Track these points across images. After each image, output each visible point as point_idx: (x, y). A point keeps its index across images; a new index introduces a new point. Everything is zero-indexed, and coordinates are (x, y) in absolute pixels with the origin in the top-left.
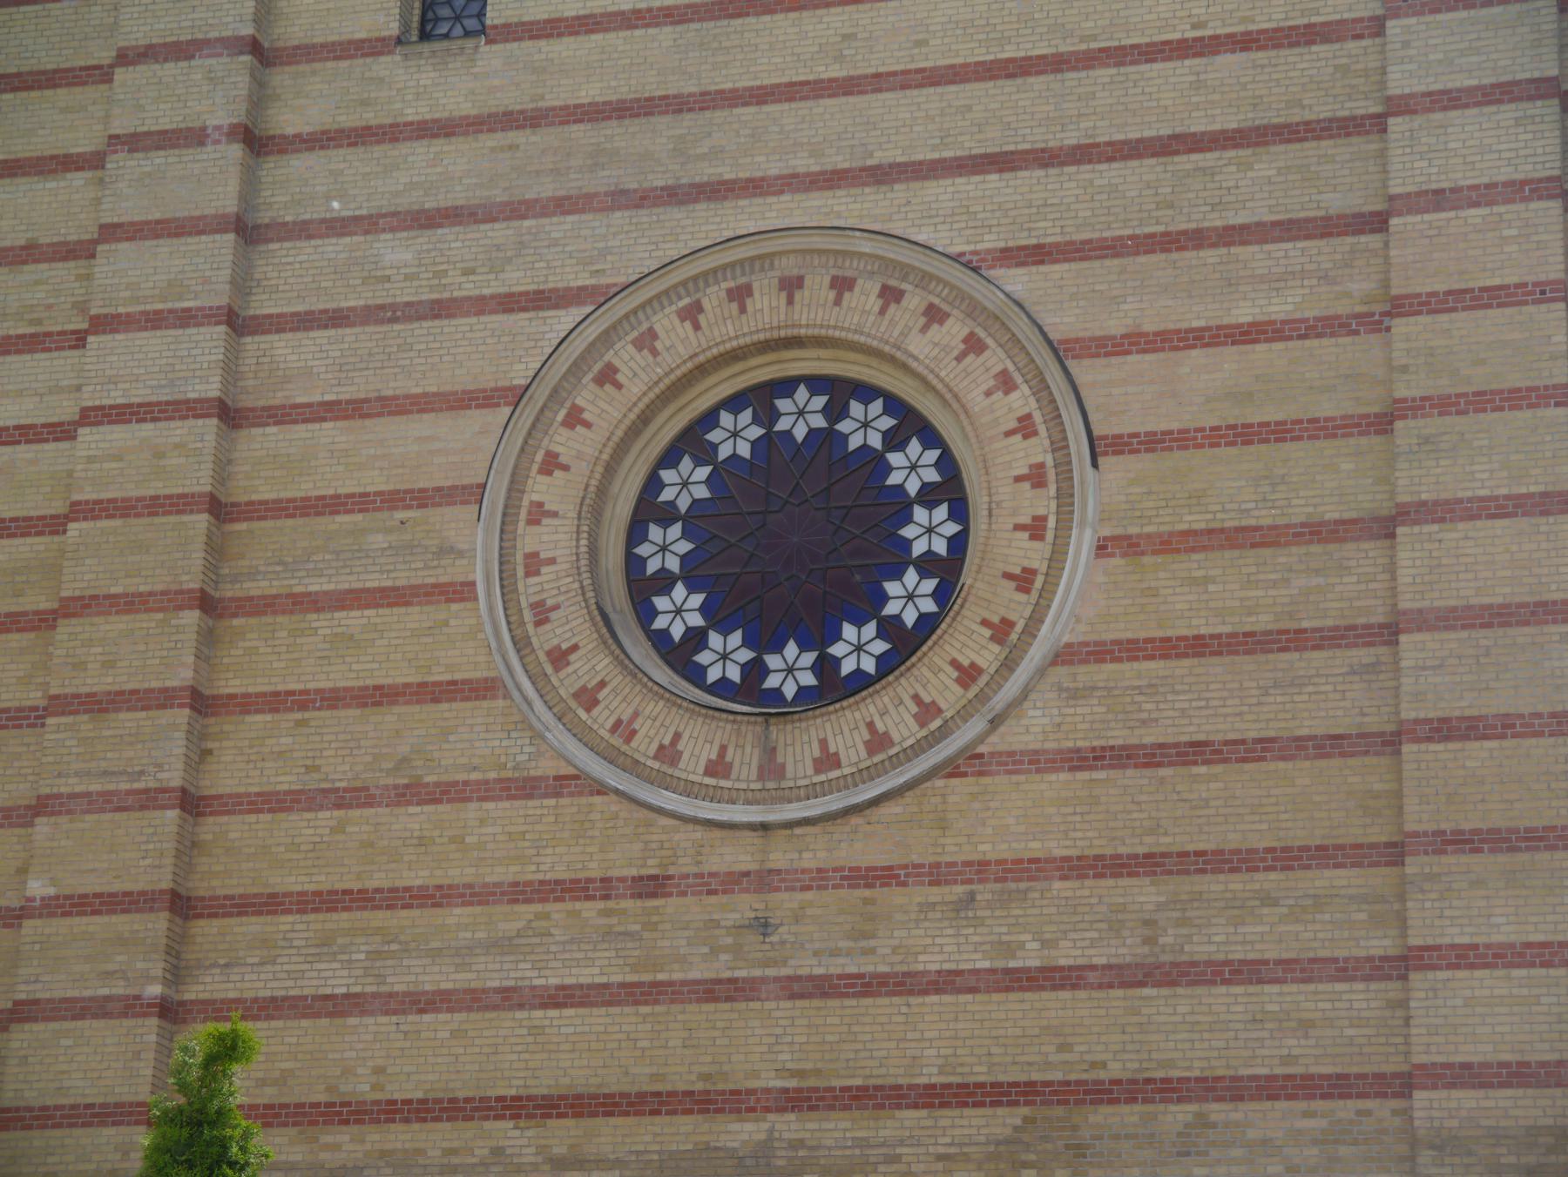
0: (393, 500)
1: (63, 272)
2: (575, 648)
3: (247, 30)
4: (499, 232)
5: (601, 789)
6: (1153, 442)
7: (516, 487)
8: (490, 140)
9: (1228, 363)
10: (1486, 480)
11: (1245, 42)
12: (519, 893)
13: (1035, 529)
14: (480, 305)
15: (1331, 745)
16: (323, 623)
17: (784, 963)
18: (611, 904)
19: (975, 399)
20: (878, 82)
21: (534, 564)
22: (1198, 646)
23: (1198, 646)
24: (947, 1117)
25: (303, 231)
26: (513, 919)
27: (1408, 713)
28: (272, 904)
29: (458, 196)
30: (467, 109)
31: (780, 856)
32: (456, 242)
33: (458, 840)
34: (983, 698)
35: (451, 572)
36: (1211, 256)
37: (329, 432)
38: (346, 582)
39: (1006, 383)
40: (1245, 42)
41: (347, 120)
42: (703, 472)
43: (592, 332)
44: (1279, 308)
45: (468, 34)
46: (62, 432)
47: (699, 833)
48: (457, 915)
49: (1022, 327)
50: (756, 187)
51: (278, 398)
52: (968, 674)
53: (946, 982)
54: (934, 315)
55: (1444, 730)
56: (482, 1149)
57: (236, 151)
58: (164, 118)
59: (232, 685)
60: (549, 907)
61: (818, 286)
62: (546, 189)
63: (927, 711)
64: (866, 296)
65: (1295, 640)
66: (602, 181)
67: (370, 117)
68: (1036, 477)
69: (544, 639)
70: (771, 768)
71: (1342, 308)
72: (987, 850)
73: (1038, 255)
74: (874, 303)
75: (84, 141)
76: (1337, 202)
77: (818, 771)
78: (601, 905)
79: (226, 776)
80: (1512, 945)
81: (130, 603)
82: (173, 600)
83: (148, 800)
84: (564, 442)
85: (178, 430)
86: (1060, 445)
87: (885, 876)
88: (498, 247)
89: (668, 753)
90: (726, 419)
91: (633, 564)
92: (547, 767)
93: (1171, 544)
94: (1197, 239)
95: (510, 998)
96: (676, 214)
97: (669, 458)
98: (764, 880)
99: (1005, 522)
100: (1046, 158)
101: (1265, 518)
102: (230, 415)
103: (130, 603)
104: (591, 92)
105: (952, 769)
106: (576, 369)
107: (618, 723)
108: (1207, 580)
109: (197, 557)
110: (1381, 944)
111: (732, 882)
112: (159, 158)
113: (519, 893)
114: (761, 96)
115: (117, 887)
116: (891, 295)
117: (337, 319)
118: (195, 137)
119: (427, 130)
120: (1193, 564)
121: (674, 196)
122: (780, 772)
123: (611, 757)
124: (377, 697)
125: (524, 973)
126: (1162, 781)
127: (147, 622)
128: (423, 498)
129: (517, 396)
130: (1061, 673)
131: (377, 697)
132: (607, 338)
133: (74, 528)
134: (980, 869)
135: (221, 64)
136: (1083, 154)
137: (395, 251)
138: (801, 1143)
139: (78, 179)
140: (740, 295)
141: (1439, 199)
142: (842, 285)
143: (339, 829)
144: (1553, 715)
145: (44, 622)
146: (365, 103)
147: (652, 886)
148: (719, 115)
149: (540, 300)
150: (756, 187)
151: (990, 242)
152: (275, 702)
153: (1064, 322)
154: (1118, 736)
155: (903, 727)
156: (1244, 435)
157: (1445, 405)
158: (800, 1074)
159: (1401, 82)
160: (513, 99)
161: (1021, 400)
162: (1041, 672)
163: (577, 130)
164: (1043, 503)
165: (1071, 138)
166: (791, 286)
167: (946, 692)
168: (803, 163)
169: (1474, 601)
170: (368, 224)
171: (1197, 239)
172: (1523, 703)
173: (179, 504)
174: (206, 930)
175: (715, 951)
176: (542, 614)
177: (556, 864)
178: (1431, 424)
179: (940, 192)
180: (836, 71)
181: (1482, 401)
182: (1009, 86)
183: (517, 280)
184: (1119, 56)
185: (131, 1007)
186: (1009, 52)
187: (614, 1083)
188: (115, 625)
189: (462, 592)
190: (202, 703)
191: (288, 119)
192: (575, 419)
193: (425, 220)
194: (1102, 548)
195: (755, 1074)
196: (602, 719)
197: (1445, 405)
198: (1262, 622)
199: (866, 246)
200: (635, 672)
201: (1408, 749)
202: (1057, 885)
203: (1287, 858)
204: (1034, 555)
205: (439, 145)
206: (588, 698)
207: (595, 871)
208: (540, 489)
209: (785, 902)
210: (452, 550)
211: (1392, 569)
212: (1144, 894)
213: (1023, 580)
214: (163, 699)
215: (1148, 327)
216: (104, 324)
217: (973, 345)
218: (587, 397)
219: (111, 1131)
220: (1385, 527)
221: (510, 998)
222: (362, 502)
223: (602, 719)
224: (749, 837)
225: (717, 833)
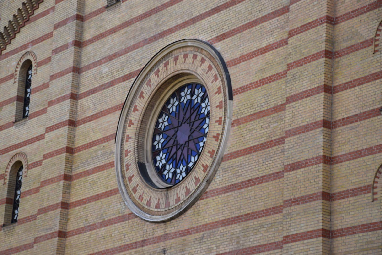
2: (133, 176)
4: (123, 58)
7: (124, 133)
8: (122, 31)
18: (137, 249)
32: (116, 62)
33: (110, 236)
36: (258, 27)
37: (92, 124)
41: (98, 33)
47: (154, 226)
50: (170, 31)
58: (61, 43)
59: (73, 199)
67: (102, 31)
70: (168, 204)
73: (222, 37)
74: (191, 60)
77: (176, 203)
78: (134, 250)
80: (304, 233)
86: (225, 95)
87: (186, 233)
88: (123, 63)
91: (153, 147)
98: (165, 237)
107: (140, 196)
108: (254, 129)
111: (159, 239)
118: (65, 47)
120: (250, 125)
121: (155, 38)
124: (98, 197)
126: (242, 193)
131: (98, 197)
137: (105, 69)
140: (166, 65)
143: (90, 237)
144: (316, 158)
148: (164, 12)
150: (170, 31)
151: (215, 35)
154: (234, 181)
160: (127, 18)
166: (176, 59)
169: (301, 125)
179: (204, 22)
183: (126, 71)
189: (111, 165)
193: (110, 58)
196: (136, 196)
198: (264, 140)
199: (190, 44)
202: (220, 229)
203: (267, 212)
212: (237, 228)
213: (216, 137)
225: (157, 225)
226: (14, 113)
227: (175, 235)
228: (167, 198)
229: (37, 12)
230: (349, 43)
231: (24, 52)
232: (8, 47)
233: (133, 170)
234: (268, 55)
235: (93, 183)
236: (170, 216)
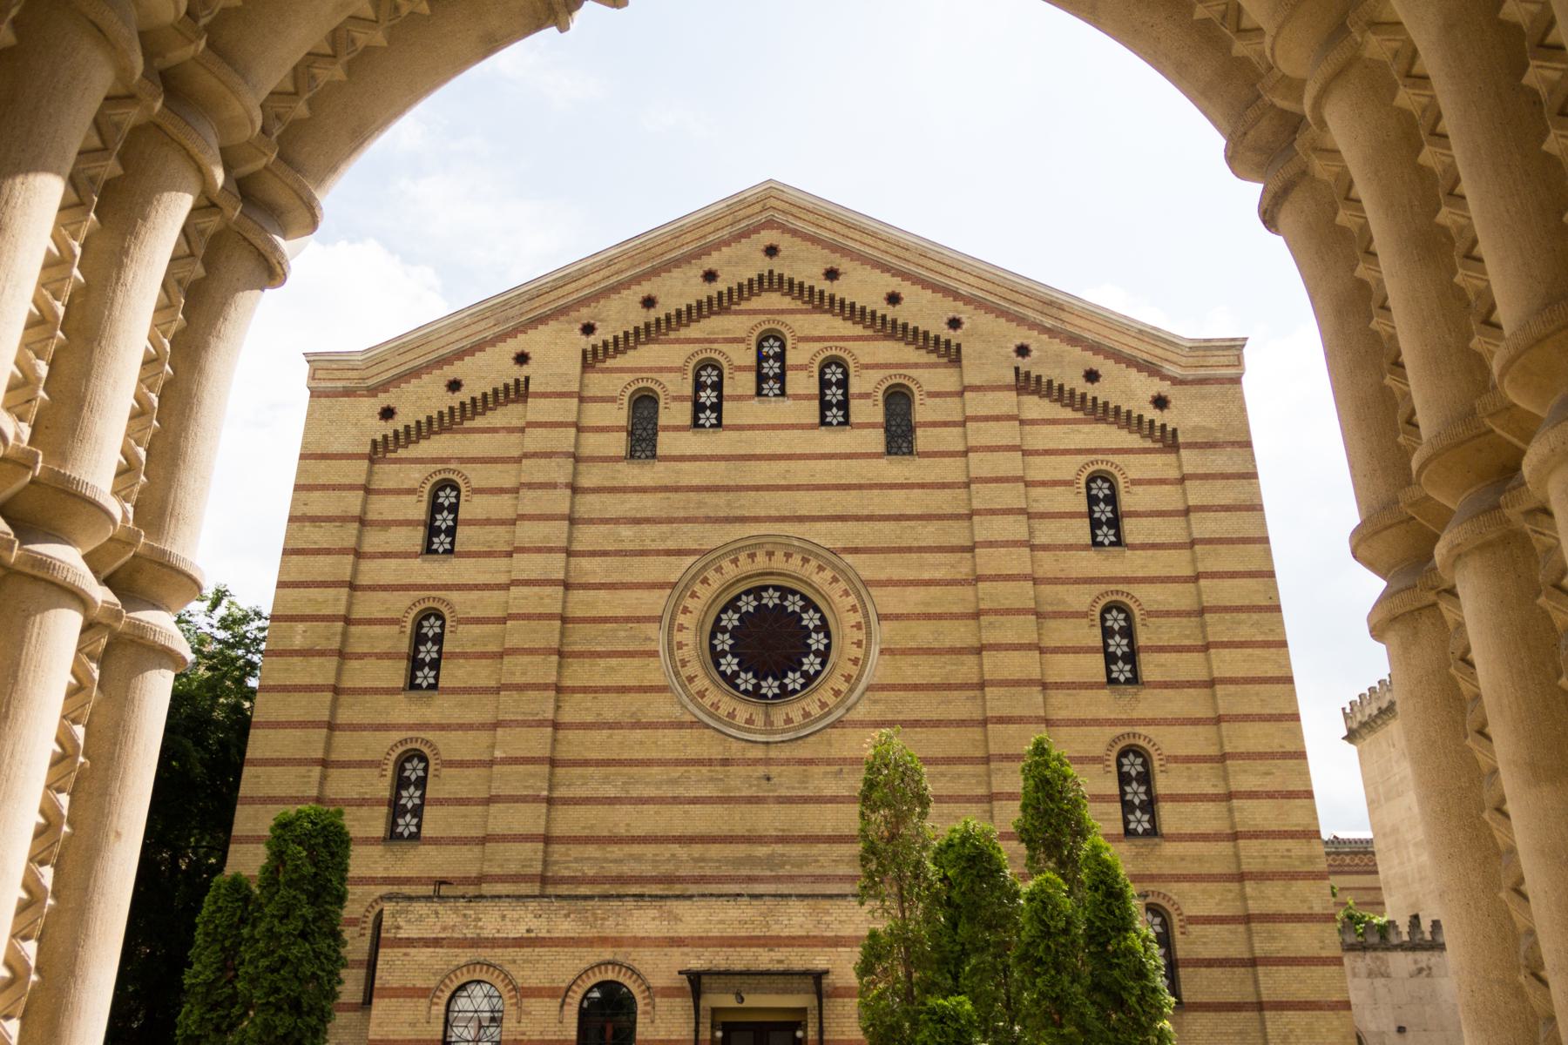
0: (627, 620)
1: (501, 529)
3: (572, 450)
4: (664, 528)
5: (707, 726)
6: (898, 617)
7: (673, 619)
9: (921, 593)
10: (1011, 638)
11: (922, 486)
12: (678, 763)
13: (859, 644)
14: (658, 553)
15: (961, 723)
16: (602, 662)
17: (775, 791)
19: (836, 598)
20: (798, 487)
21: (680, 645)
22: (916, 687)
23: (916, 687)
24: (835, 847)
25: (591, 521)
26: (677, 772)
27: (989, 714)
28: (586, 763)
29: (649, 514)
30: (651, 484)
31: (773, 753)
32: (650, 530)
34: (843, 701)
35: (650, 647)
36: (914, 556)
38: (610, 648)
39: (846, 593)
40: (922, 486)
41: (607, 484)
42: (736, 616)
43: (699, 565)
44: (938, 575)
45: (647, 457)
46: (505, 587)
47: (743, 744)
48: (655, 770)
49: (851, 575)
50: (756, 519)
51: (583, 580)
52: (837, 693)
53: (834, 800)
54: (821, 569)
55: (1001, 720)
56: (667, 855)
57: (568, 492)
58: (540, 477)
59: (568, 683)
60: (690, 768)
61: (779, 555)
62: (682, 514)
63: (823, 705)
64: (796, 560)
65: (948, 687)
66: (701, 513)
67: (615, 483)
68: (858, 626)
69: (685, 672)
70: (769, 722)
71: (959, 577)
72: (846, 754)
73: (855, 551)
74: (799, 563)
75: (509, 482)
76: (955, 541)
79: (567, 716)
81: (531, 652)
82: (547, 651)
83: (540, 724)
84: (689, 602)
85: (548, 590)
86: (866, 615)
87: (810, 762)
89: (732, 715)
90: (744, 598)
92: (687, 718)
93: (905, 652)
94: (910, 550)
95: (676, 800)
96: (728, 526)
97: (724, 610)
98: (767, 762)
99: (848, 641)
100: (857, 518)
101: (936, 645)
102: (567, 586)
103: (531, 652)
104: (696, 482)
105: (832, 726)
106: (694, 577)
108: (918, 665)
109: (557, 636)
110: (981, 791)
112: (539, 492)
113: (678, 763)
114: (757, 488)
115: (529, 755)
116: (805, 560)
117: (605, 553)
118: (554, 486)
119: (636, 490)
120: (913, 659)
121: (728, 520)
122: (772, 724)
123: (711, 715)
125: (680, 791)
127: (538, 659)
128: (638, 620)
129: (673, 586)
130: (869, 694)
132: (704, 568)
133: (509, 623)
134: (844, 761)
135: (561, 461)
136: (870, 518)
137: (626, 532)
138: (783, 855)
139: (506, 496)
140: (752, 556)
141: (991, 544)
142: (788, 556)
143: (610, 736)
145: (500, 655)
146: (613, 478)
147: (725, 762)
148: (743, 494)
149: (680, 553)
150: (756, 519)
151: (839, 545)
152: (585, 690)
153: (866, 574)
155: (815, 711)
156: (928, 617)
157: (996, 612)
158: (783, 830)
159: (976, 504)
161: (852, 600)
162: (863, 693)
163: (692, 494)
164: (861, 635)
165: (866, 512)
166: (770, 554)
167: (831, 700)
168: (773, 513)
170: (616, 521)
171: (910, 550)
172: (1026, 713)
173: (550, 617)
174: (560, 771)
175: (751, 786)
176: (684, 663)
177: (692, 752)
178: (992, 618)
180: (783, 482)
181: (1008, 612)
182: (844, 493)
183: (671, 545)
184: (881, 486)
185: (536, 799)
186: (843, 482)
187: (715, 832)
188: (526, 659)
189: (654, 654)
190: (559, 689)
191: (585, 481)
192: (693, 595)
194: (882, 652)
195: (766, 830)
196: (707, 702)
197: (996, 612)
198: (936, 680)
199: (796, 543)
200: (718, 686)
201: (989, 726)
203: (949, 761)
204: (859, 653)
205: (641, 495)
206: (702, 694)
207: (706, 756)
208: (681, 619)
209: (774, 770)
210: (649, 639)
211: (981, 665)
213: (855, 661)
214: (546, 687)
215: (895, 578)
216: (521, 550)
217: (835, 580)
218: (698, 587)
219: (529, 844)
220: (979, 650)
221: (676, 800)
222: (615, 620)
223: (707, 702)
224: (761, 746)
226: (420, 542)
227: (788, 762)
228: (767, 715)
229: (467, 424)
230: (1055, 608)
231: (439, 466)
232: (400, 451)
233: (694, 668)
234: (935, 591)
235: (612, 669)
236: (778, 738)
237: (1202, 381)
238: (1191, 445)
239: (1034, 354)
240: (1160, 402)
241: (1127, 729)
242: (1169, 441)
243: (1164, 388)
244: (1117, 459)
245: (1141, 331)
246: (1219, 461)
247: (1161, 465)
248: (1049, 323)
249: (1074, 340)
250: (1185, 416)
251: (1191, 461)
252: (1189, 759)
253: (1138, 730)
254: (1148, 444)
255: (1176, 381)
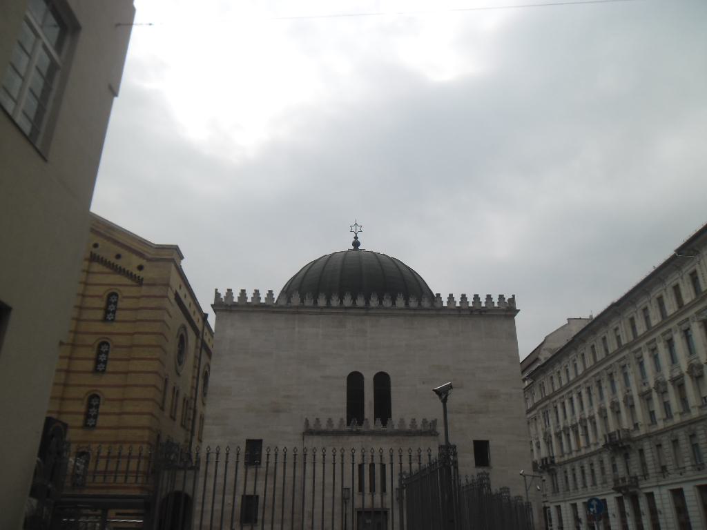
237: (158, 260)
238: (148, 285)
239: (100, 247)
240: (140, 268)
241: (95, 389)
242: (139, 282)
243: (143, 262)
244: (118, 288)
245: (140, 241)
246: (156, 291)
247: (134, 291)
248: (108, 235)
249: (116, 242)
250: (149, 273)
251: (144, 290)
252: (113, 400)
253: (99, 389)
254: (134, 283)
255: (149, 260)
